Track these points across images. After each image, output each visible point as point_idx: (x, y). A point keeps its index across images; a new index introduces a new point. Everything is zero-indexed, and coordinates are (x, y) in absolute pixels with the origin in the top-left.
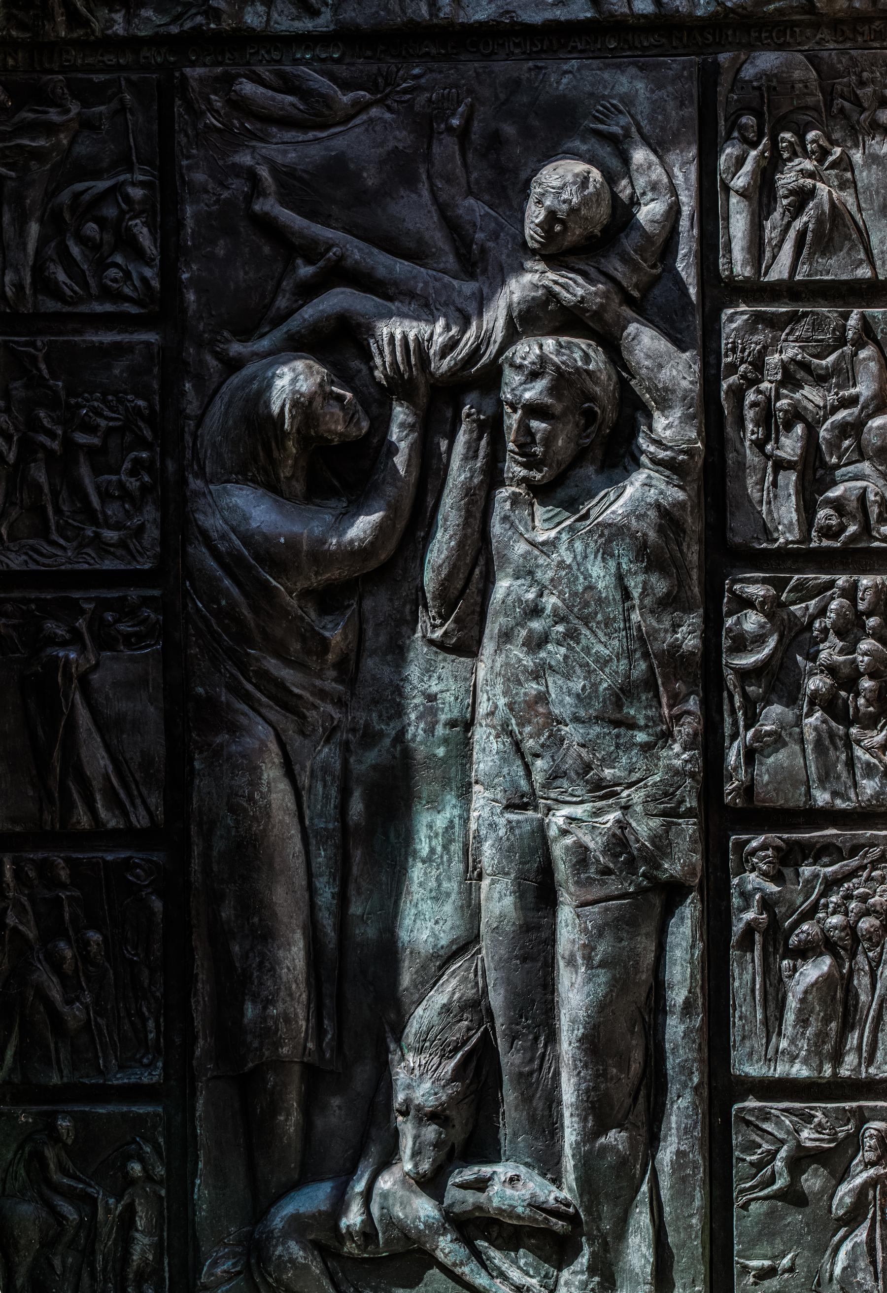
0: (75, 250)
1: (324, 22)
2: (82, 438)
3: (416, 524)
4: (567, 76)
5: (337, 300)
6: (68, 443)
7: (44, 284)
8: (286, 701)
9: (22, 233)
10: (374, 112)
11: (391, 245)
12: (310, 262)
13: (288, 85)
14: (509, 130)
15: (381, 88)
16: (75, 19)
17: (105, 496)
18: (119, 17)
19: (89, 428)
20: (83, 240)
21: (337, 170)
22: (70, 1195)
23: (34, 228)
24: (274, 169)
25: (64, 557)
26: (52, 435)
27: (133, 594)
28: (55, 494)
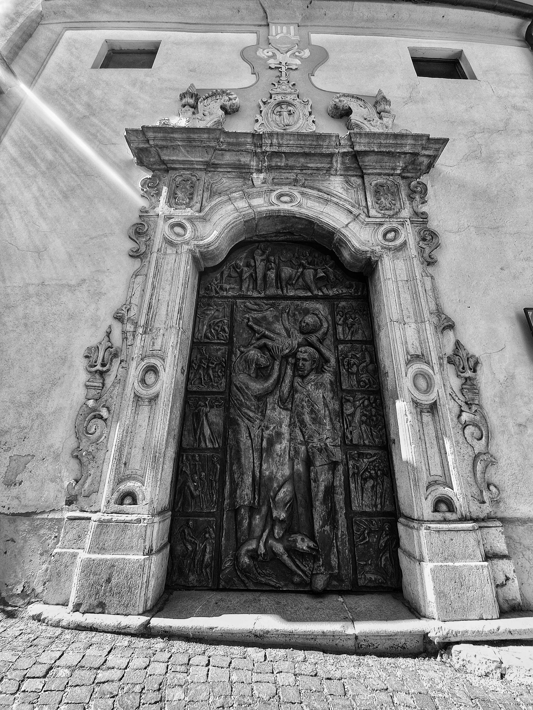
0: (213, 331)
1: (262, 295)
2: (210, 365)
3: (279, 381)
4: (307, 304)
5: (263, 341)
6: (208, 366)
7: (206, 337)
8: (249, 419)
9: (203, 328)
10: (271, 309)
11: (273, 332)
12: (259, 334)
13: (256, 304)
14: (297, 313)
15: (272, 305)
16: (217, 292)
17: (214, 377)
18: (225, 293)
19: (213, 364)
20: (214, 329)
21: (264, 318)
22: (191, 543)
23: (205, 327)
24: (252, 318)
25: (205, 389)
26: (205, 364)
27: (219, 397)
28: (204, 376)
